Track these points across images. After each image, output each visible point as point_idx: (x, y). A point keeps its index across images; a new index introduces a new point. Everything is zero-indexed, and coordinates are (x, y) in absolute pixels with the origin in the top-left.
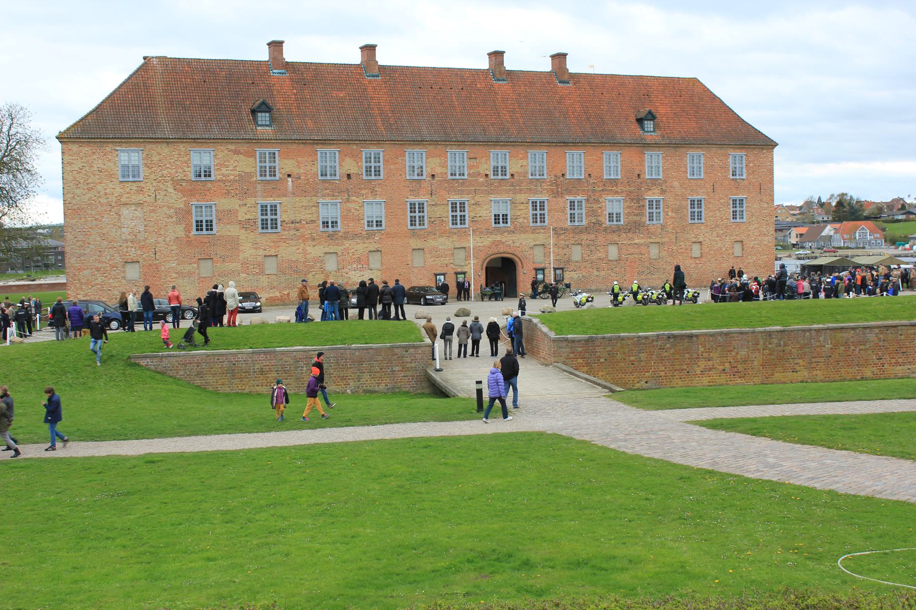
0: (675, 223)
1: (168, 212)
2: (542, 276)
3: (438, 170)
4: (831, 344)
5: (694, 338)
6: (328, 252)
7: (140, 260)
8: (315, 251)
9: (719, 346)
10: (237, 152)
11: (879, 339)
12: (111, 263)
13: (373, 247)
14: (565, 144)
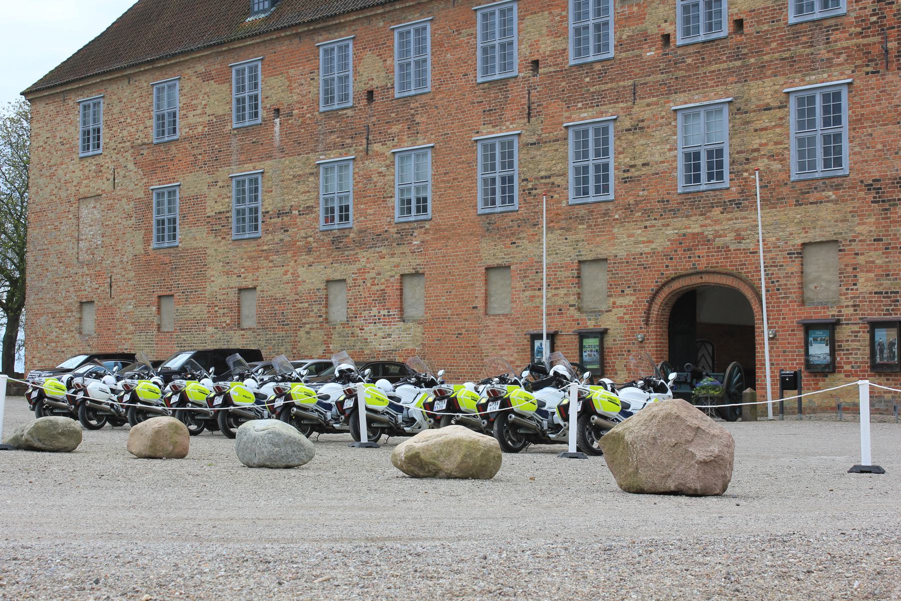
2: (826, 349)
3: (546, 46)
6: (332, 277)
10: (206, 77)
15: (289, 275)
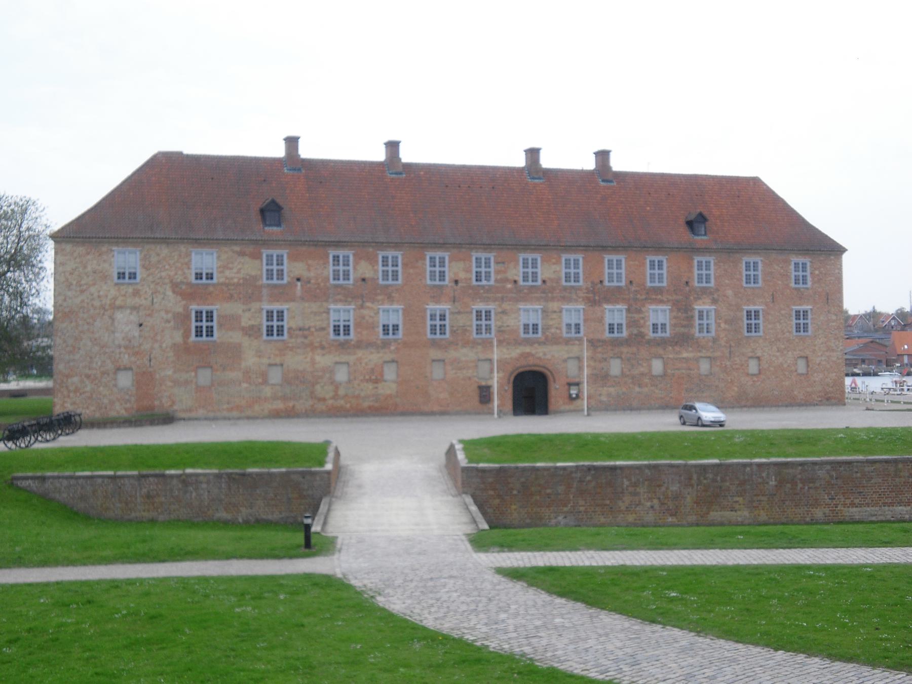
1: (165, 317)
3: (462, 275)
4: (776, 480)
5: (619, 471)
7: (134, 367)
8: (324, 360)
9: (646, 480)
10: (242, 254)
11: (831, 477)
12: (102, 369)
13: (388, 357)
14: (604, 248)
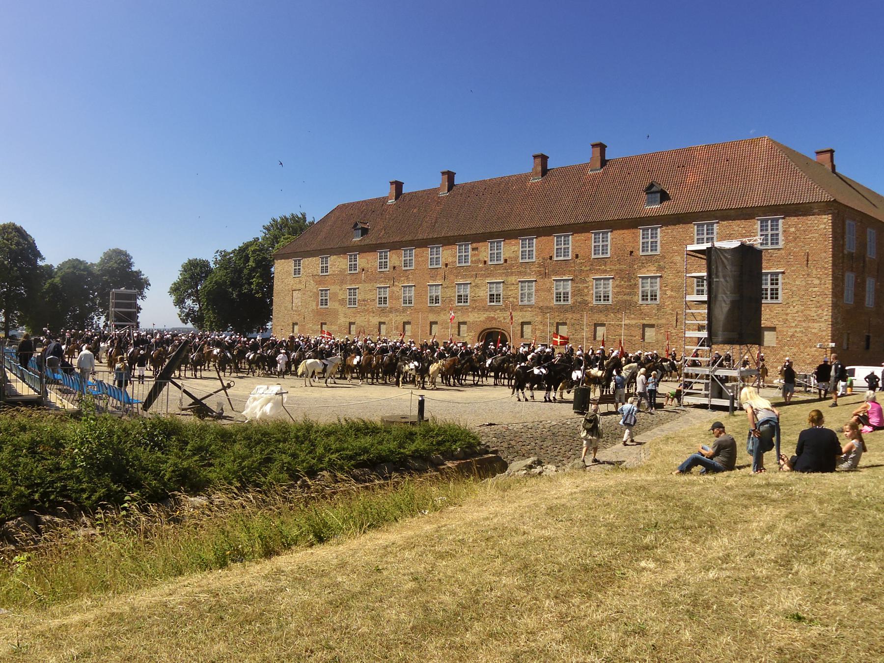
0: (675, 303)
3: (450, 260)
15: (366, 320)
